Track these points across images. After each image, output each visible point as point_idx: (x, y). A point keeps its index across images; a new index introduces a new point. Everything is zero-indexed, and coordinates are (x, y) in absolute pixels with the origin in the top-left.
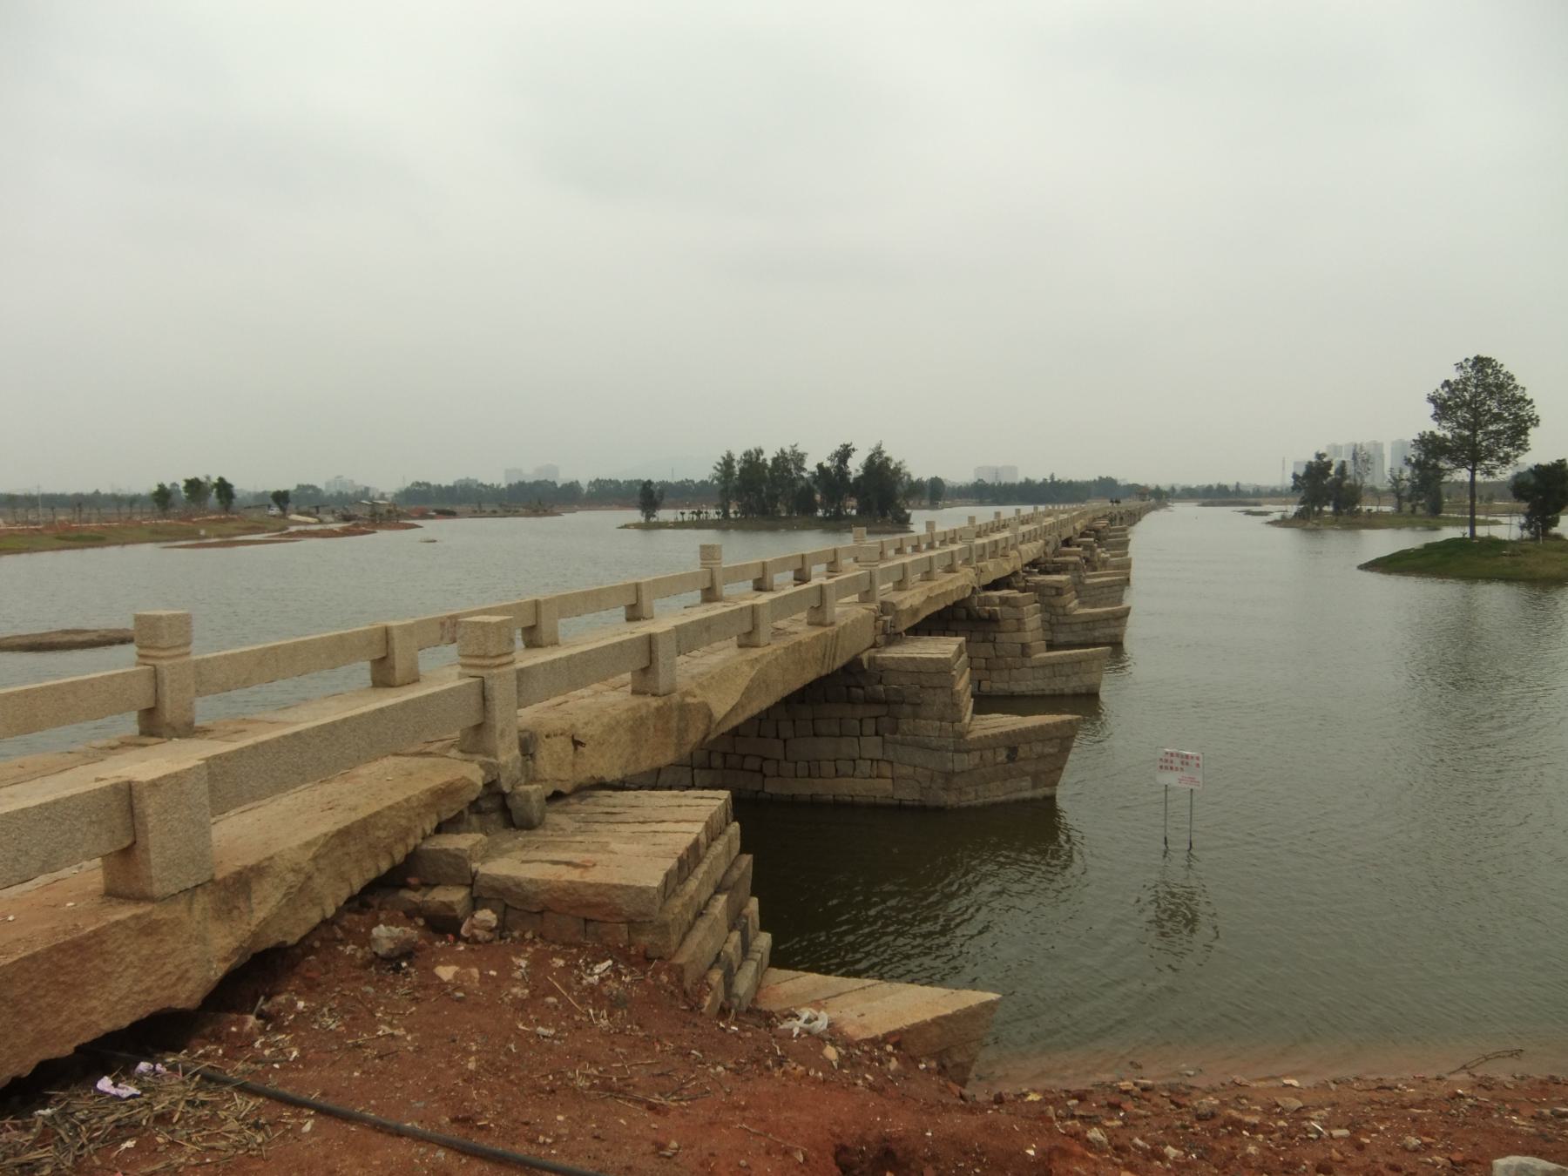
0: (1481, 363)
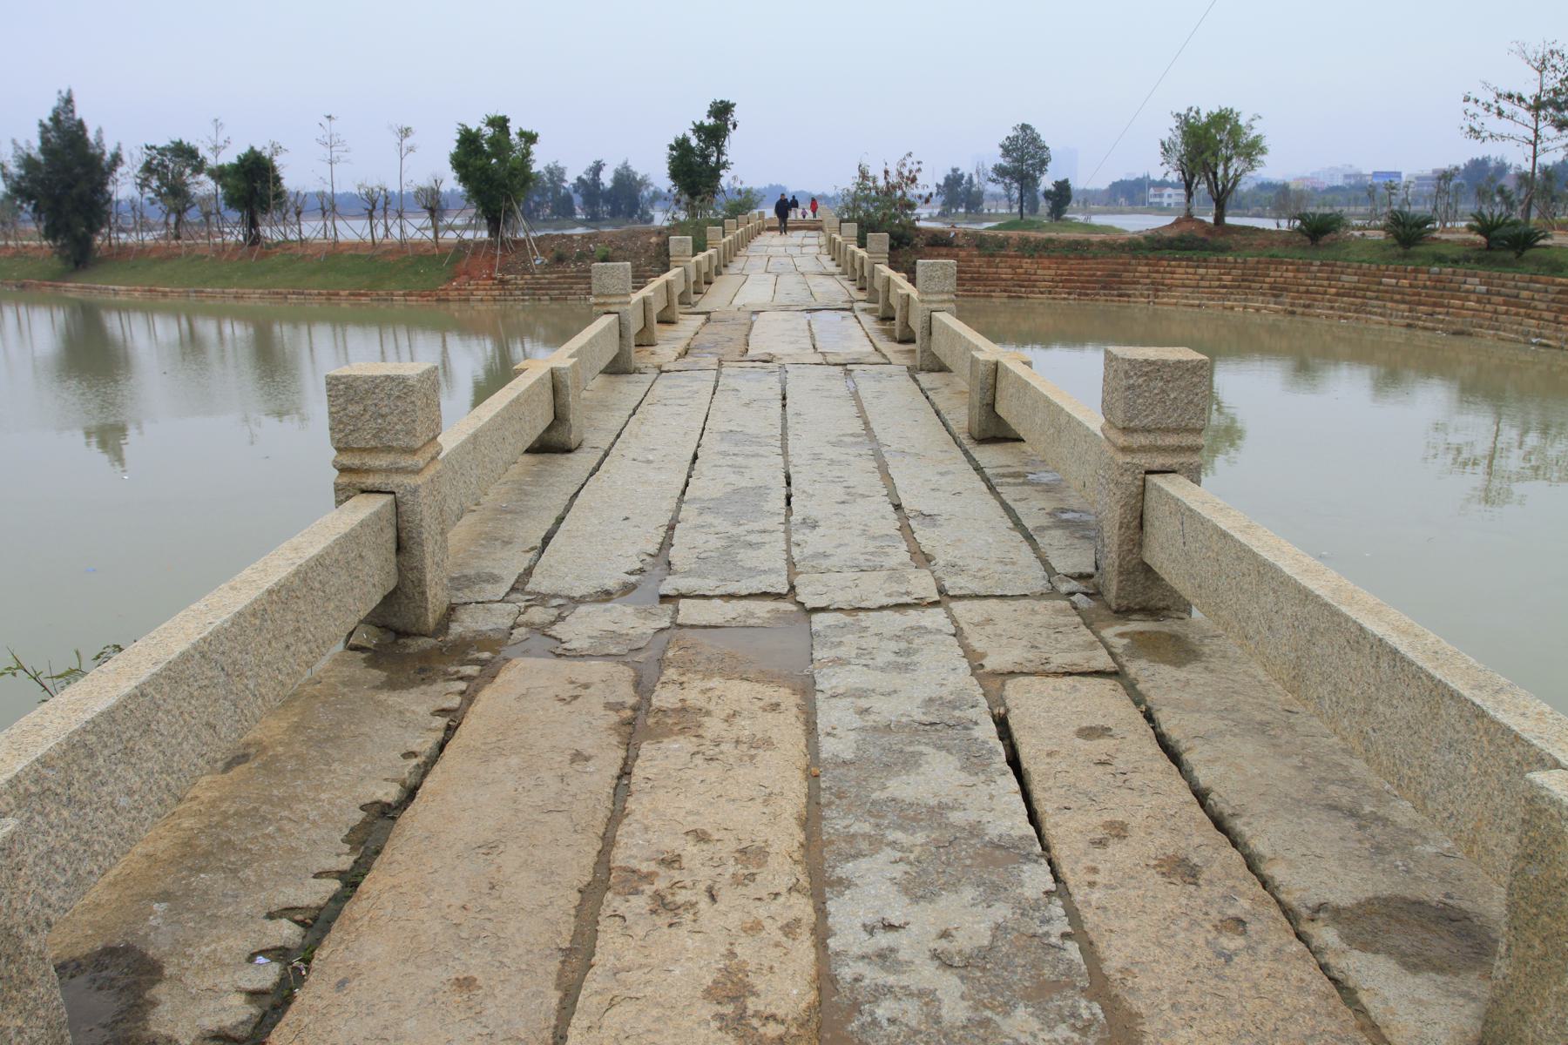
0: (1025, 127)
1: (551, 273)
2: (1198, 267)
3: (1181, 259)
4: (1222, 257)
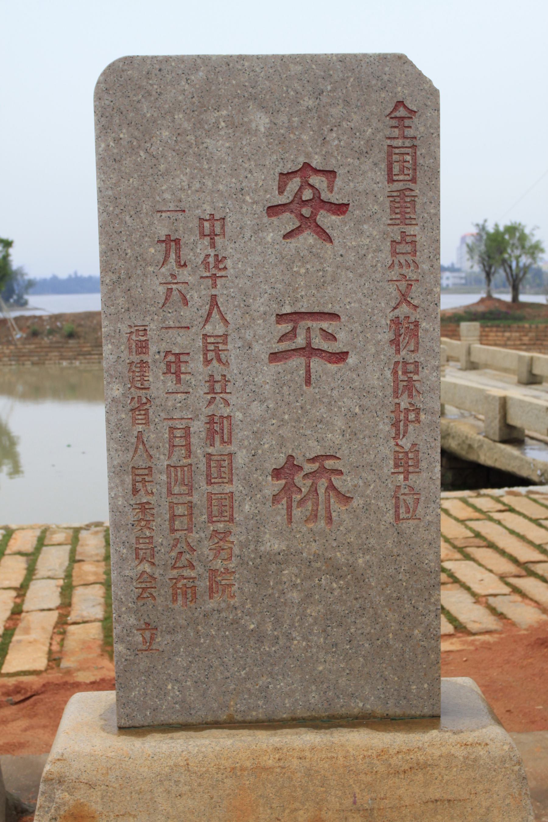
1: (30, 344)
2: (504, 331)
3: (492, 326)
4: (521, 324)
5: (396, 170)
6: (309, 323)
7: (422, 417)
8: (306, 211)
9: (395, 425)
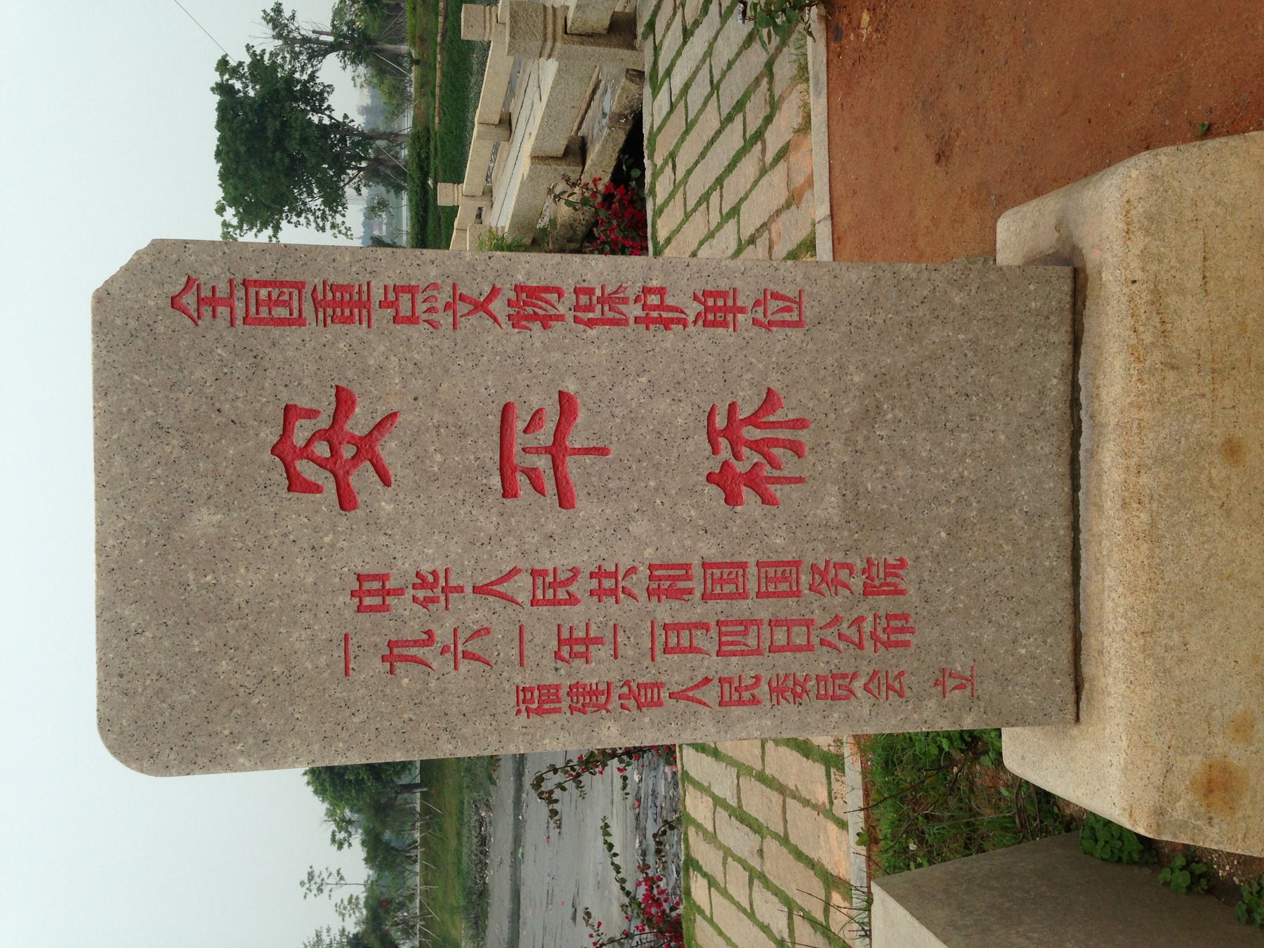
5: (281, 312)
6: (517, 449)
7: (655, 283)
8: (348, 452)
9: (667, 324)
